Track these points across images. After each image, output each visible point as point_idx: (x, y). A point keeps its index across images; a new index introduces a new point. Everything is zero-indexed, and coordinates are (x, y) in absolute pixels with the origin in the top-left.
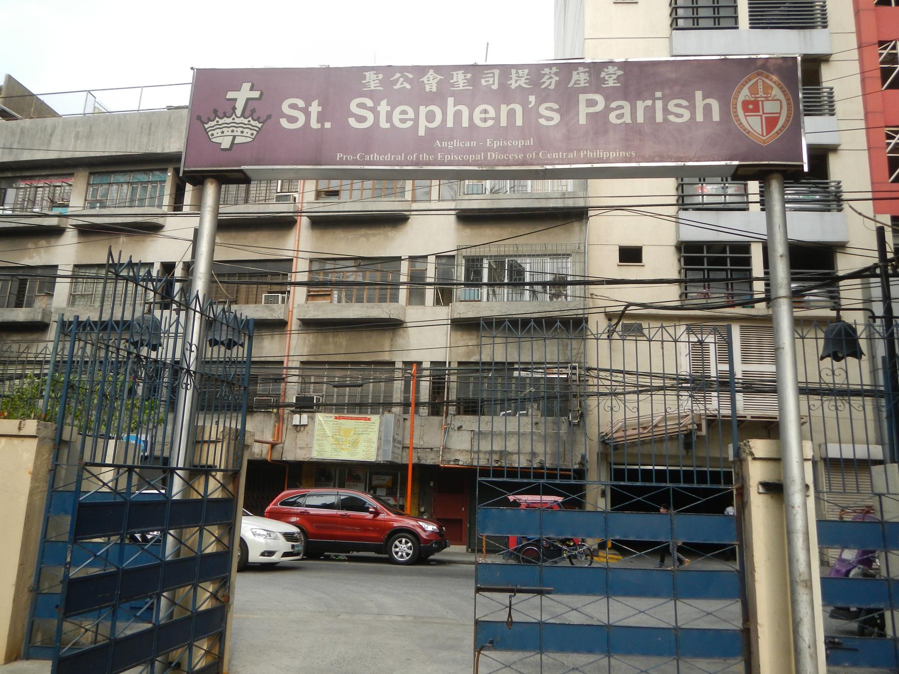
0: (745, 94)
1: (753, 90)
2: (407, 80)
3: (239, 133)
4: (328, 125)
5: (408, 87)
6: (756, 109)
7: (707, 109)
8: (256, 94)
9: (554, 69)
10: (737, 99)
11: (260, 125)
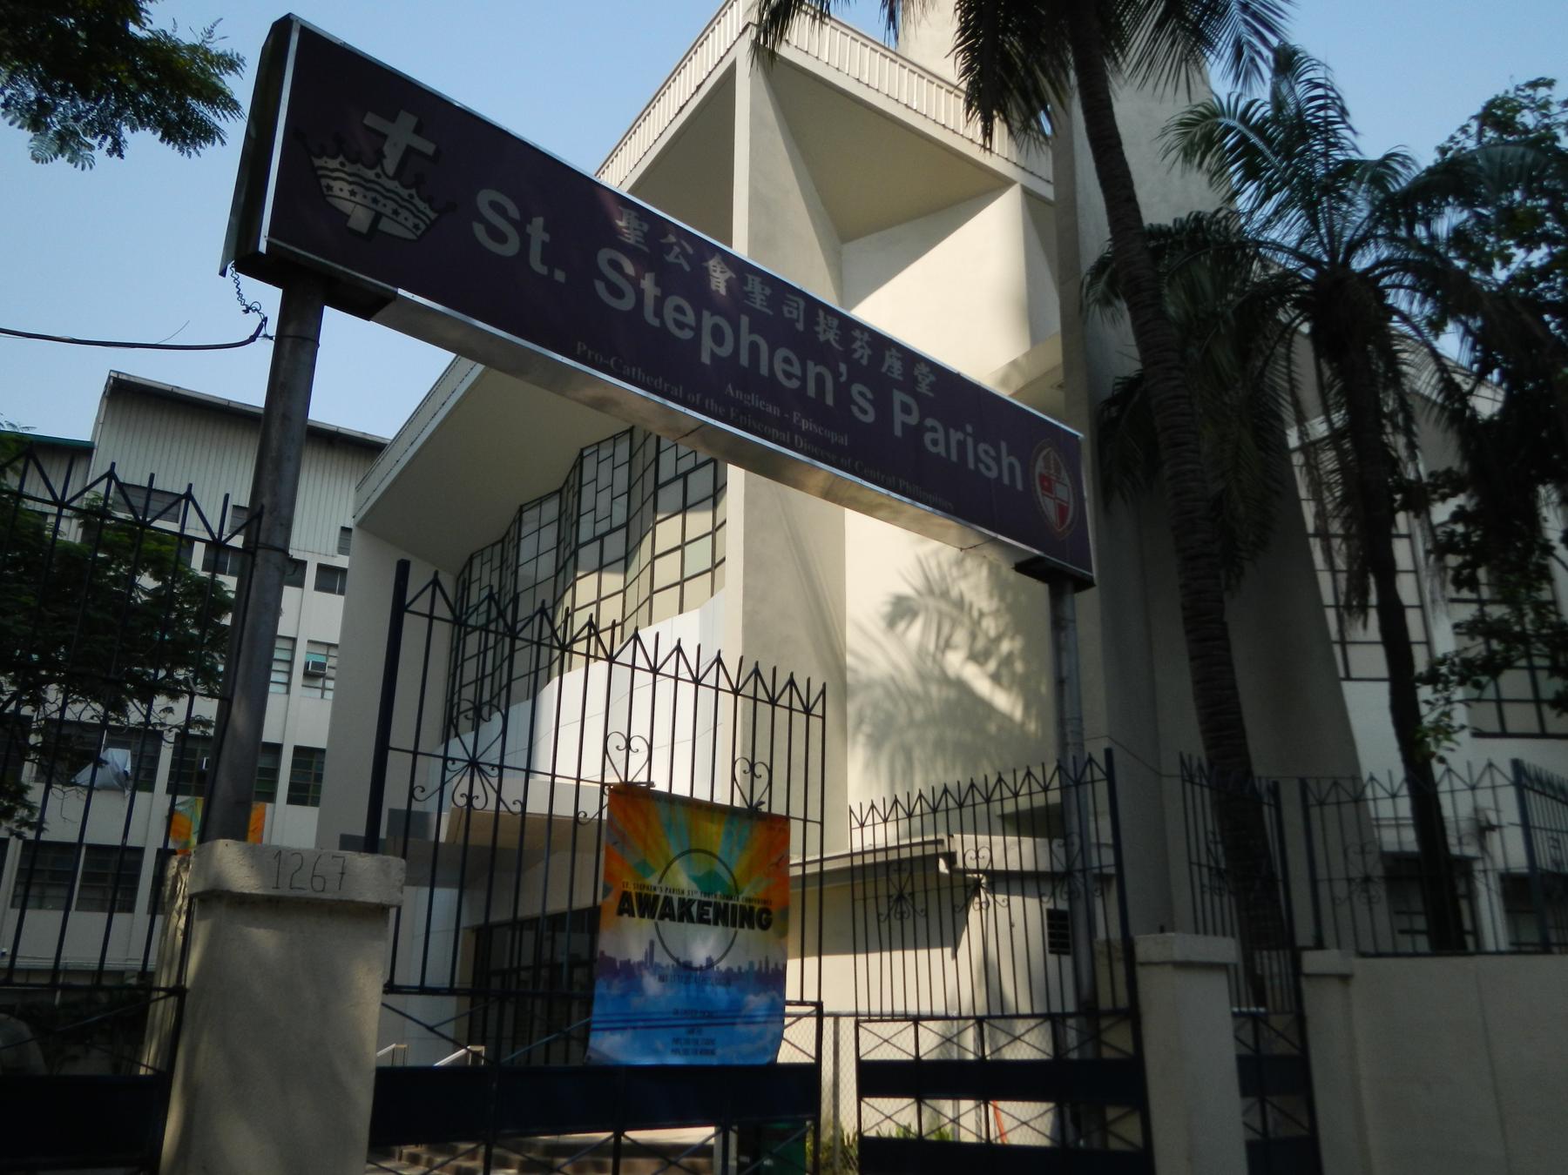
0: (1039, 467)
3: (388, 211)
5: (687, 268)
8: (429, 148)
11: (433, 216)
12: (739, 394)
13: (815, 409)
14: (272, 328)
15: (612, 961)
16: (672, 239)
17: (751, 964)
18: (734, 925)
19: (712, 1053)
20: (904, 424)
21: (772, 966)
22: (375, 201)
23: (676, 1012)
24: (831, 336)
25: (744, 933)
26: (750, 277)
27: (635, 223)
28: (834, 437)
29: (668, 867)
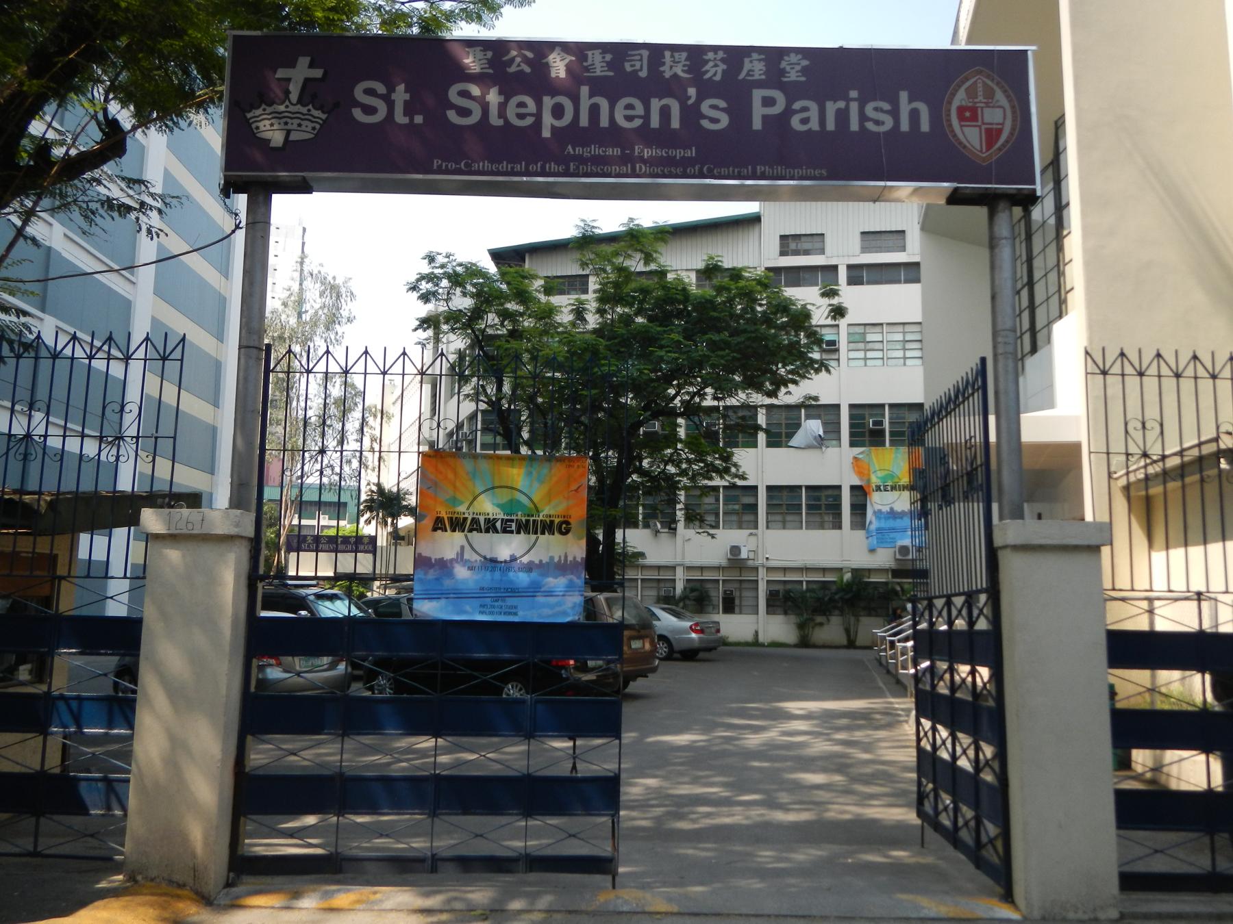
0: (960, 98)
1: (971, 93)
2: (526, 60)
3: (295, 126)
4: (419, 119)
5: (527, 69)
6: (974, 118)
7: (914, 115)
8: (318, 73)
9: (721, 54)
10: (950, 103)
11: (324, 116)
12: (579, 150)
13: (663, 137)
14: (243, 224)
15: (430, 559)
16: (514, 53)
17: (552, 558)
18: (536, 533)
19: (515, 614)
20: (765, 118)
21: (570, 558)
22: (286, 123)
23: (482, 589)
24: (679, 70)
25: (544, 538)
26: (590, 53)
27: (480, 55)
28: (679, 153)
29: (475, 499)
